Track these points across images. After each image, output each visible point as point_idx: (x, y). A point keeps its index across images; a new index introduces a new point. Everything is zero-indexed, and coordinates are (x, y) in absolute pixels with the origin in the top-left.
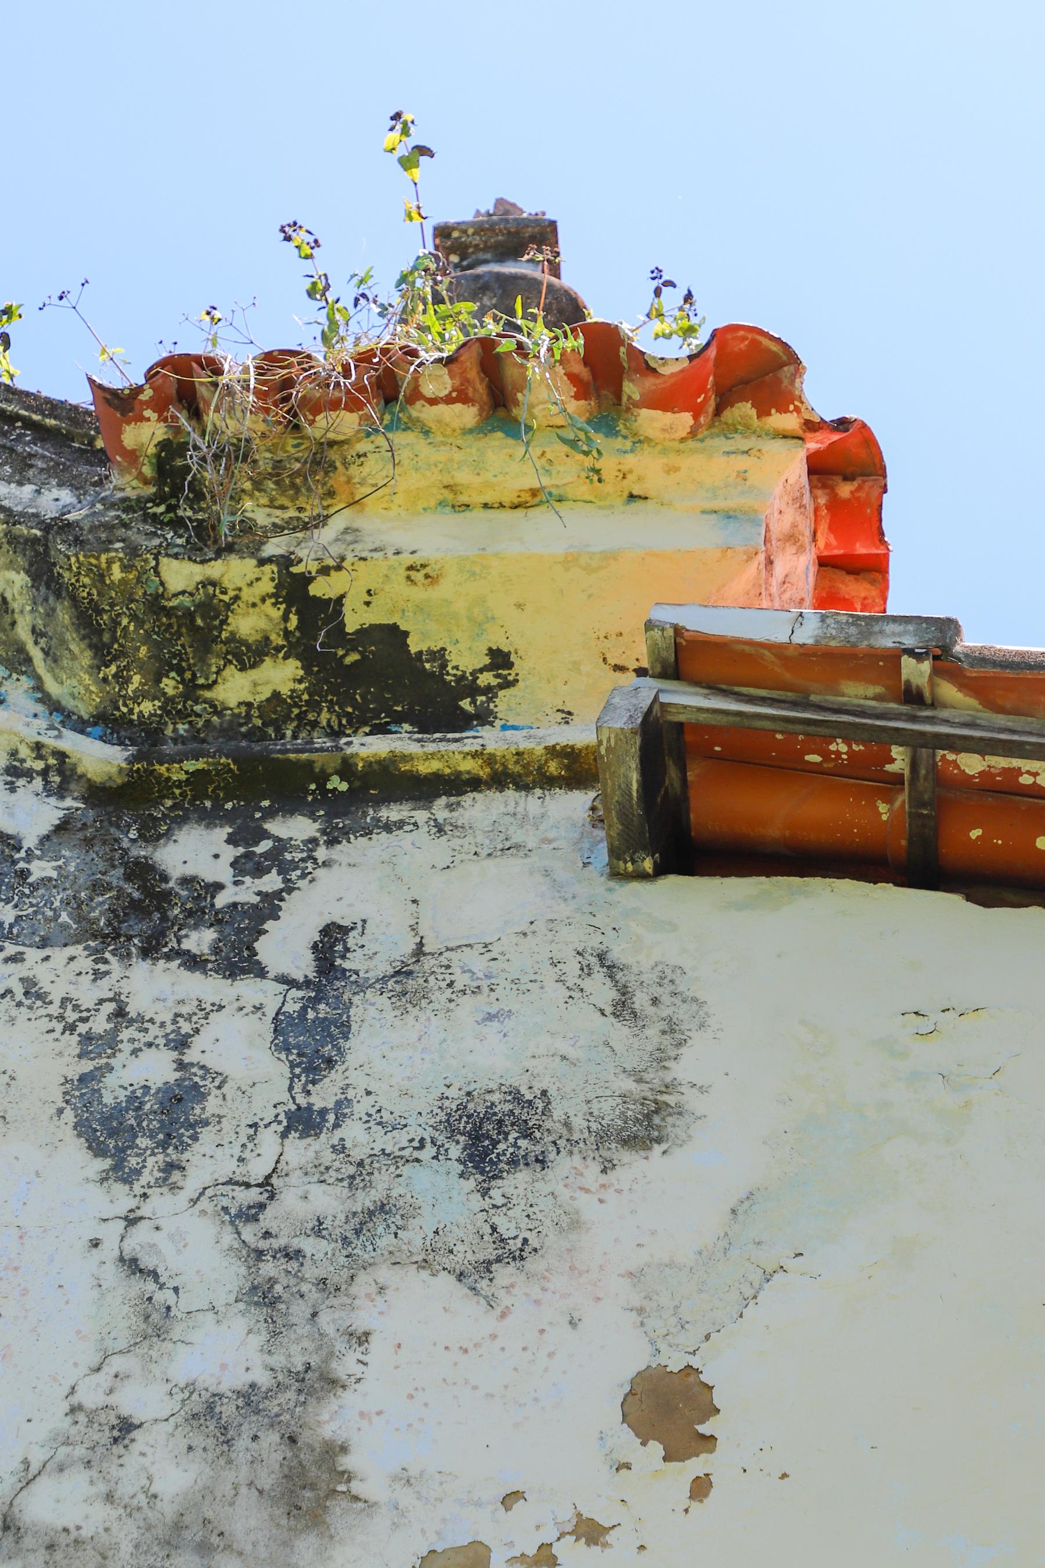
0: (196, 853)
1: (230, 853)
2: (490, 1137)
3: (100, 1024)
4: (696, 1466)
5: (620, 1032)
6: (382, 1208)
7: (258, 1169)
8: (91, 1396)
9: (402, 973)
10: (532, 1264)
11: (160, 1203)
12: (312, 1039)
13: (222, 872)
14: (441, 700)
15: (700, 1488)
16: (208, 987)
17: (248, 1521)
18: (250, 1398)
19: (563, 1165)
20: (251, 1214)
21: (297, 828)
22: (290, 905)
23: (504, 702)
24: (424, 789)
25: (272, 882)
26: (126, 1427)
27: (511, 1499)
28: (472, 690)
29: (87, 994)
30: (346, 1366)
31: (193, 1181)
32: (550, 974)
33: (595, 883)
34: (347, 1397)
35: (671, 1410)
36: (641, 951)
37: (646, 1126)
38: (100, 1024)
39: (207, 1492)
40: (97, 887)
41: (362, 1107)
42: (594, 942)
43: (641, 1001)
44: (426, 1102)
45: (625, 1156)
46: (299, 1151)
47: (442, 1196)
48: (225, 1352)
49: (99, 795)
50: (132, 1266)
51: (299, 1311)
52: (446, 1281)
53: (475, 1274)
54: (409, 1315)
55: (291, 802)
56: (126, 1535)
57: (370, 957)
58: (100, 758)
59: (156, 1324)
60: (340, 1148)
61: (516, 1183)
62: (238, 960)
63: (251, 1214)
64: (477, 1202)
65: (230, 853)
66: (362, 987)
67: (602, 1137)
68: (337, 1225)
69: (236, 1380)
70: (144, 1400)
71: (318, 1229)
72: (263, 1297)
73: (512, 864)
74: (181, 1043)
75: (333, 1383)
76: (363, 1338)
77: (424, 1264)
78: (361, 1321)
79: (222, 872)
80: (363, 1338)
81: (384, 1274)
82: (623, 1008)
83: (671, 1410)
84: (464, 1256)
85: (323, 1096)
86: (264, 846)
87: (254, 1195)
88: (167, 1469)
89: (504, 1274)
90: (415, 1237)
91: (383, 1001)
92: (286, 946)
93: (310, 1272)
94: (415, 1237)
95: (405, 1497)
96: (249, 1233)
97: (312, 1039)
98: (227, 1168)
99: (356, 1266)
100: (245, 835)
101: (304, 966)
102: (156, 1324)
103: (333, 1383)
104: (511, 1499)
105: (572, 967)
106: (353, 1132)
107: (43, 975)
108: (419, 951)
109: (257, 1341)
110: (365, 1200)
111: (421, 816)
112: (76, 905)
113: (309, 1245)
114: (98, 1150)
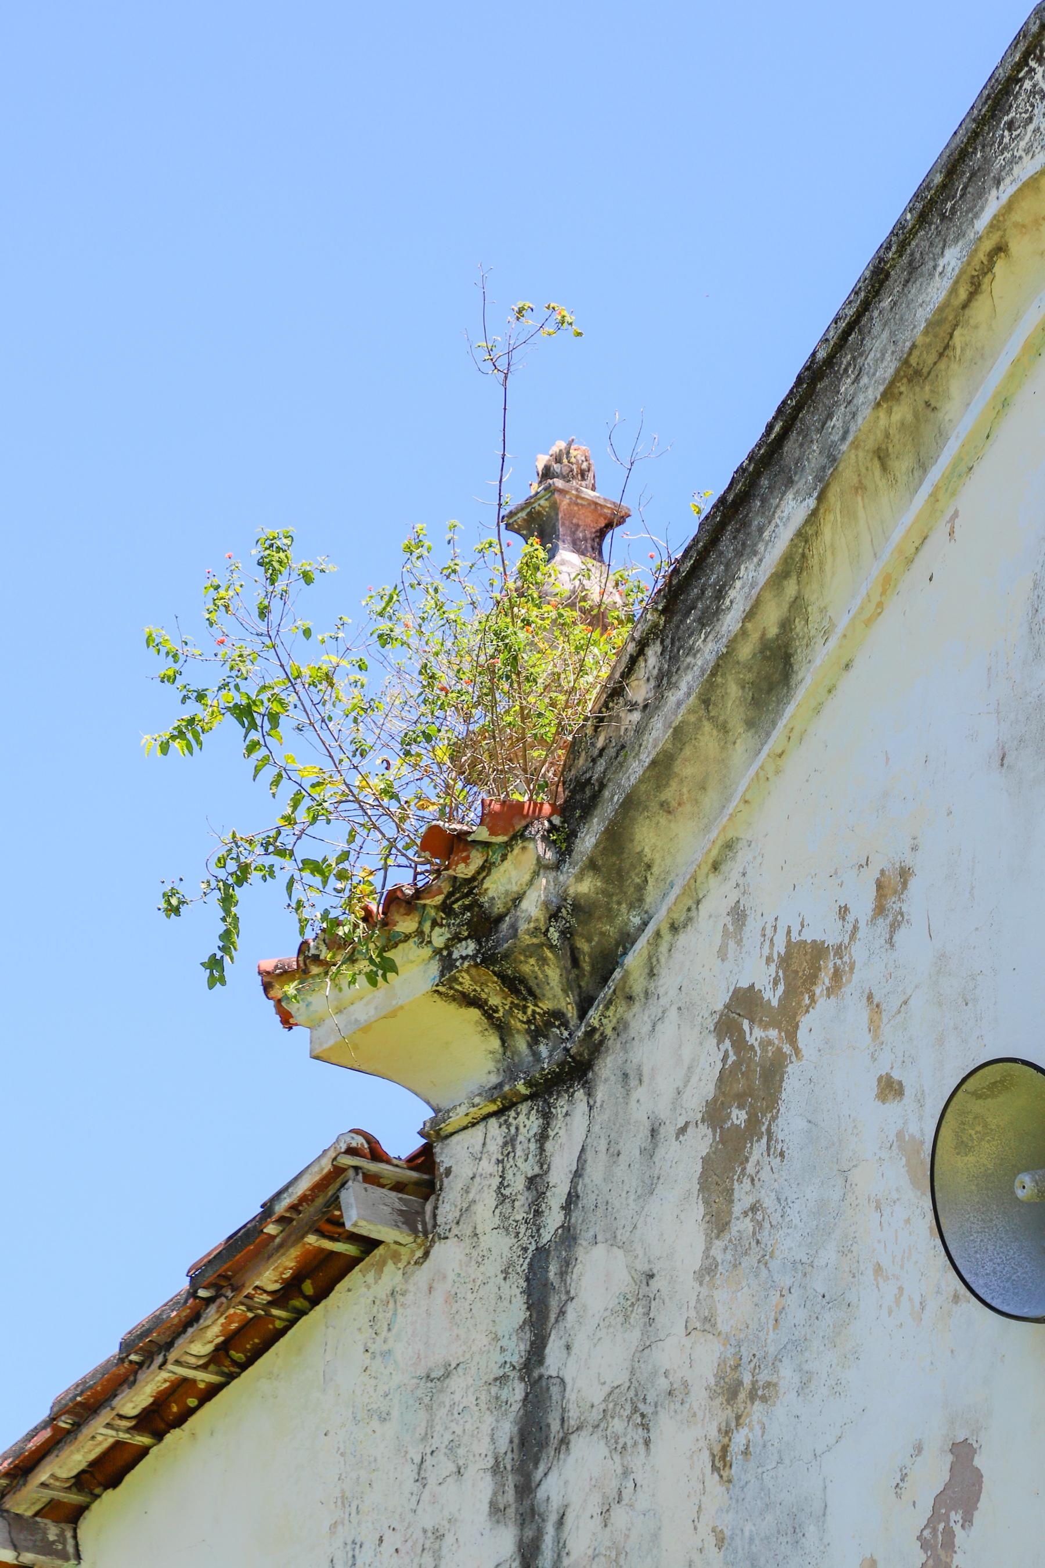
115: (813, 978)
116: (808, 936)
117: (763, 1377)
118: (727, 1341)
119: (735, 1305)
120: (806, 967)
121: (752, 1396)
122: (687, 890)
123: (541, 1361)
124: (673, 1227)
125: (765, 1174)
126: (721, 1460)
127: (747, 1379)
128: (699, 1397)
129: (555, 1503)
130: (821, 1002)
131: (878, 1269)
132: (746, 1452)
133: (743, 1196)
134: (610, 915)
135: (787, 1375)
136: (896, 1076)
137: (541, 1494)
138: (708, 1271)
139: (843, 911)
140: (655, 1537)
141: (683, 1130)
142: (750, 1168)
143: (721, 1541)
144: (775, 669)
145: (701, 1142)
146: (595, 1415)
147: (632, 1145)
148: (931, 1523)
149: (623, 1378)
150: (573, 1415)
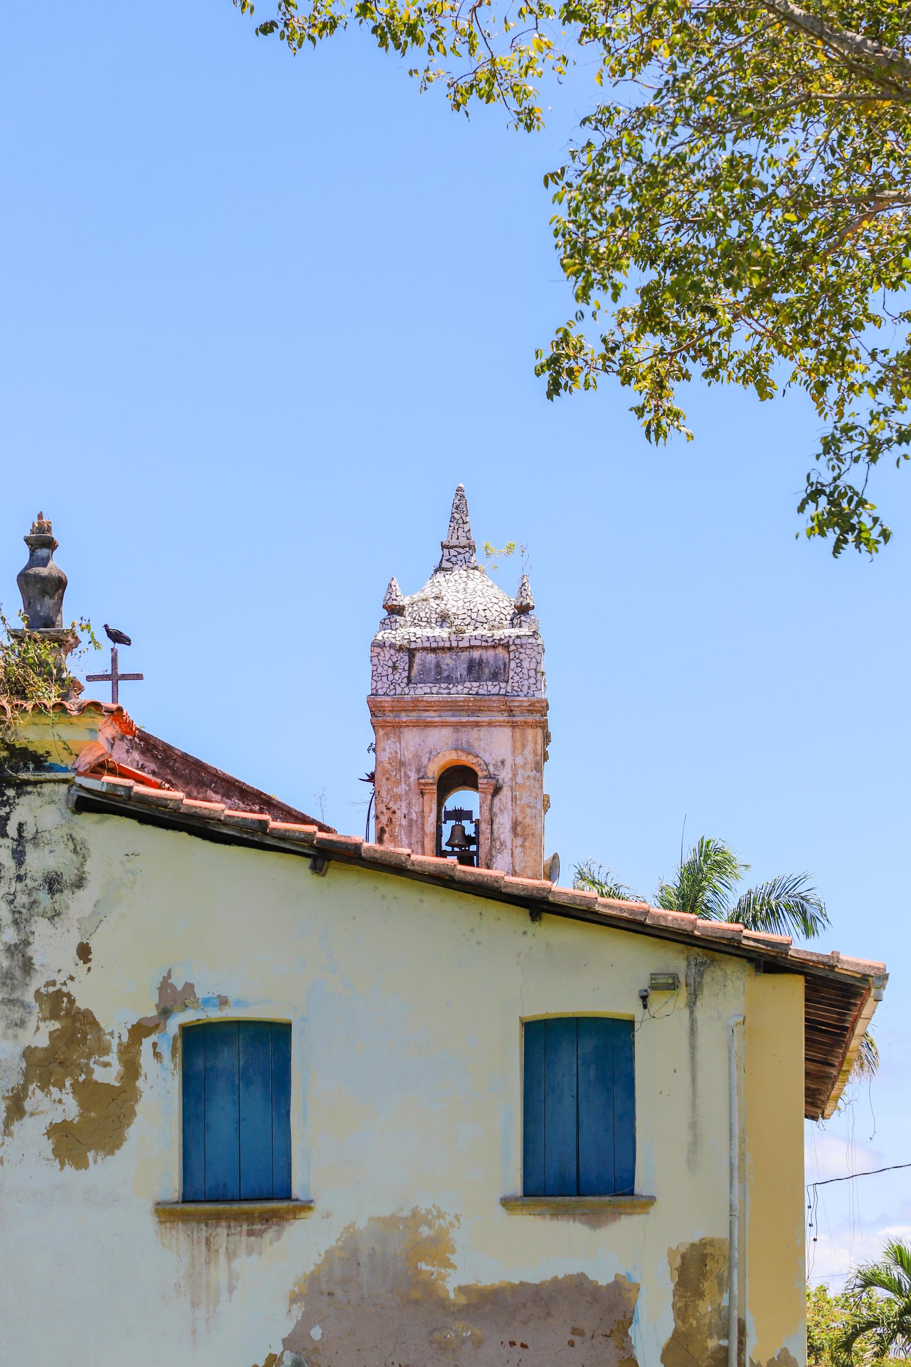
2: (53, 883)
4: (88, 965)
5: (74, 857)
6: (34, 902)
7: (12, 890)
9: (34, 838)
10: (61, 917)
12: (19, 856)
14: (39, 761)
15: (89, 969)
17: (18, 973)
18: (16, 945)
19: (66, 892)
20: (12, 902)
22: (12, 816)
23: (49, 759)
24: (35, 783)
25: (7, 809)
27: (59, 971)
28: (42, 756)
30: (31, 940)
32: (61, 841)
33: (69, 814)
34: (32, 947)
35: (84, 952)
36: (79, 835)
37: (79, 883)
39: (11, 966)
41: (29, 875)
42: (69, 832)
43: (78, 848)
44: (40, 874)
45: (76, 890)
46: (20, 886)
47: (43, 896)
51: (22, 926)
52: (46, 920)
53: (51, 918)
54: (40, 926)
57: (28, 834)
60: (26, 886)
61: (57, 896)
63: (12, 902)
64: (51, 901)
66: (27, 842)
67: (72, 885)
68: (27, 905)
69: (12, 942)
71: (24, 907)
72: (16, 922)
73: (52, 807)
75: (29, 944)
76: (33, 933)
77: (43, 916)
78: (33, 929)
80: (33, 933)
82: (75, 851)
83: (84, 952)
84: (50, 914)
85: (22, 873)
86: (5, 798)
87: (12, 897)
89: (56, 918)
90: (41, 909)
91: (31, 846)
93: (24, 917)
94: (41, 909)
95: (43, 969)
96: (12, 907)
97: (19, 856)
98: (7, 890)
99: (32, 916)
101: (16, 836)
103: (29, 944)
104: (59, 971)
105: (65, 839)
106: (28, 881)
108: (37, 832)
109: (16, 933)
110: (32, 899)
111: (35, 790)
113: (23, 910)
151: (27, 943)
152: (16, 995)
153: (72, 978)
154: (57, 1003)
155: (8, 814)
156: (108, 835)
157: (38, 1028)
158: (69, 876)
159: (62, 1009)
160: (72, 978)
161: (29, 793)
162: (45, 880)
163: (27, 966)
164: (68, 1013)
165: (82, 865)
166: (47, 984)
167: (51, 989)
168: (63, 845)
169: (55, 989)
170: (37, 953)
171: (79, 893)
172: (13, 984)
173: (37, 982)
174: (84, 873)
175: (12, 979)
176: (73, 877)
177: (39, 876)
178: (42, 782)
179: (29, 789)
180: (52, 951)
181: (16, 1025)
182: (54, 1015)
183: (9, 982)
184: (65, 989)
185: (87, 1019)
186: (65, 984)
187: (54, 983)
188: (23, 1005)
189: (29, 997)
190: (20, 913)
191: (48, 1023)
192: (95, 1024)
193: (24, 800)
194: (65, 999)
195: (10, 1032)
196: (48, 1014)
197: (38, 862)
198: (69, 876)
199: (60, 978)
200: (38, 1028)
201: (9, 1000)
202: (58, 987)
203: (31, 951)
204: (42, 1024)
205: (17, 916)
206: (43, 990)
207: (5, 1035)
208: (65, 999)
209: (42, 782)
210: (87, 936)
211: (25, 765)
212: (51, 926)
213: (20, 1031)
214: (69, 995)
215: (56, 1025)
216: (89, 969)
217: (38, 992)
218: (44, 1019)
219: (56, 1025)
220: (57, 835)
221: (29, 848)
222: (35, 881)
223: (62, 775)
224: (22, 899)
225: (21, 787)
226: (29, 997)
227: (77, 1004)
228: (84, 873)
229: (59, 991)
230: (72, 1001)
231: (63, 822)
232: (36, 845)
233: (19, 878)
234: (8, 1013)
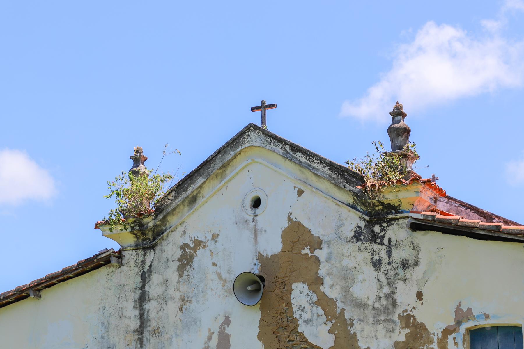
0: (377, 229)
1: (380, 228)
2: (404, 265)
3: (372, 252)
5: (414, 252)
6: (397, 274)
8: (378, 295)
11: (380, 273)
12: (389, 253)
13: (379, 231)
15: (422, 303)
16: (380, 247)
17: (390, 307)
18: (389, 294)
19: (410, 268)
20: (386, 274)
21: (385, 225)
22: (386, 235)
25: (384, 232)
26: (380, 297)
27: (409, 305)
29: (371, 248)
30: (396, 291)
31: (382, 270)
35: (419, 295)
38: (372, 252)
40: (370, 234)
44: (399, 261)
47: (400, 271)
48: (386, 290)
49: (367, 221)
50: (378, 280)
51: (391, 285)
54: (400, 285)
55: (384, 222)
56: (382, 308)
57: (393, 243)
58: (367, 218)
59: (381, 287)
61: (407, 270)
62: (382, 244)
63: (386, 274)
65: (380, 228)
69: (387, 293)
70: (381, 295)
72: (389, 284)
73: (403, 229)
74: (379, 254)
75: (395, 293)
76: (396, 288)
78: (396, 286)
79: (379, 231)
81: (397, 281)
83: (419, 295)
84: (403, 279)
87: (386, 272)
88: (384, 302)
89: (406, 281)
90: (399, 277)
92: (386, 241)
94: (399, 277)
97: (389, 253)
100: (381, 226)
102: (381, 287)
103: (395, 293)
104: (409, 305)
106: (394, 264)
107: (366, 245)
110: (395, 273)
112: (368, 236)
114: (374, 267)
115: (200, 245)
116: (199, 239)
117: (189, 299)
118: (182, 293)
119: (184, 288)
120: (198, 244)
121: (187, 301)
122: (175, 227)
123: (144, 288)
124: (172, 274)
125: (190, 271)
126: (181, 309)
127: (186, 299)
128: (176, 299)
129: (147, 309)
130: (201, 249)
131: (212, 289)
132: (186, 309)
133: (185, 273)
134: (161, 227)
135: (194, 300)
136: (216, 263)
137: (144, 307)
138: (179, 282)
139: (206, 237)
140: (168, 317)
141: (174, 261)
142: (187, 269)
143: (181, 320)
144: (193, 200)
145: (177, 264)
146: (156, 298)
147: (163, 261)
148: (221, 325)
149: (161, 294)
150: (151, 297)
151: (394, 293)
152: (390, 317)
153: (414, 308)
154: (408, 320)
155: (384, 234)
156: (428, 240)
157: (400, 332)
158: (411, 261)
159: (410, 323)
160: (414, 308)
161: (393, 224)
162: (401, 264)
163: (394, 304)
164: (413, 325)
165: (417, 255)
166: (404, 311)
167: (405, 314)
168: (408, 247)
169: (407, 313)
170: (399, 297)
171: (417, 268)
172: (388, 312)
173: (399, 311)
174: (418, 259)
175: (388, 310)
176: (413, 261)
177: (398, 261)
178: (398, 219)
179: (393, 222)
180: (405, 296)
181: (390, 331)
182: (407, 326)
183: (386, 311)
184: (411, 314)
185: (422, 327)
186: (411, 311)
187: (406, 311)
188: (394, 322)
189: (396, 318)
190: (390, 279)
191: (404, 330)
192: (426, 329)
193: (391, 227)
194: (412, 318)
195: (388, 335)
196: (404, 326)
197: (398, 255)
198: (411, 261)
199: (409, 308)
200: (400, 332)
201: (387, 320)
202: (408, 312)
203: (396, 296)
204: (401, 330)
205: (389, 280)
206: (402, 314)
207: (385, 336)
208: (412, 318)
209: (398, 219)
210: (421, 288)
211: (391, 212)
212: (404, 285)
213: (392, 334)
214: (413, 316)
215: (408, 331)
216: (422, 303)
217: (399, 315)
218: (403, 328)
219: (408, 331)
220: (405, 242)
221: (393, 249)
222: (397, 264)
223: (406, 215)
224: (391, 273)
225: (389, 222)
226: (396, 318)
227: (417, 320)
228: (418, 259)
229: (409, 314)
230: (415, 319)
231: (408, 236)
232: (397, 248)
233: (390, 263)
234: (386, 325)
